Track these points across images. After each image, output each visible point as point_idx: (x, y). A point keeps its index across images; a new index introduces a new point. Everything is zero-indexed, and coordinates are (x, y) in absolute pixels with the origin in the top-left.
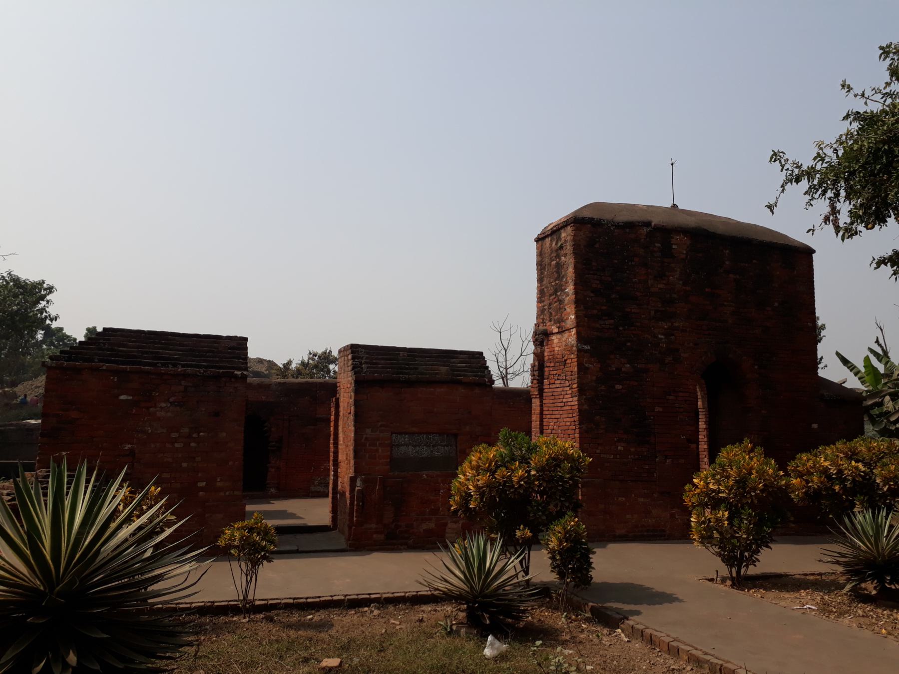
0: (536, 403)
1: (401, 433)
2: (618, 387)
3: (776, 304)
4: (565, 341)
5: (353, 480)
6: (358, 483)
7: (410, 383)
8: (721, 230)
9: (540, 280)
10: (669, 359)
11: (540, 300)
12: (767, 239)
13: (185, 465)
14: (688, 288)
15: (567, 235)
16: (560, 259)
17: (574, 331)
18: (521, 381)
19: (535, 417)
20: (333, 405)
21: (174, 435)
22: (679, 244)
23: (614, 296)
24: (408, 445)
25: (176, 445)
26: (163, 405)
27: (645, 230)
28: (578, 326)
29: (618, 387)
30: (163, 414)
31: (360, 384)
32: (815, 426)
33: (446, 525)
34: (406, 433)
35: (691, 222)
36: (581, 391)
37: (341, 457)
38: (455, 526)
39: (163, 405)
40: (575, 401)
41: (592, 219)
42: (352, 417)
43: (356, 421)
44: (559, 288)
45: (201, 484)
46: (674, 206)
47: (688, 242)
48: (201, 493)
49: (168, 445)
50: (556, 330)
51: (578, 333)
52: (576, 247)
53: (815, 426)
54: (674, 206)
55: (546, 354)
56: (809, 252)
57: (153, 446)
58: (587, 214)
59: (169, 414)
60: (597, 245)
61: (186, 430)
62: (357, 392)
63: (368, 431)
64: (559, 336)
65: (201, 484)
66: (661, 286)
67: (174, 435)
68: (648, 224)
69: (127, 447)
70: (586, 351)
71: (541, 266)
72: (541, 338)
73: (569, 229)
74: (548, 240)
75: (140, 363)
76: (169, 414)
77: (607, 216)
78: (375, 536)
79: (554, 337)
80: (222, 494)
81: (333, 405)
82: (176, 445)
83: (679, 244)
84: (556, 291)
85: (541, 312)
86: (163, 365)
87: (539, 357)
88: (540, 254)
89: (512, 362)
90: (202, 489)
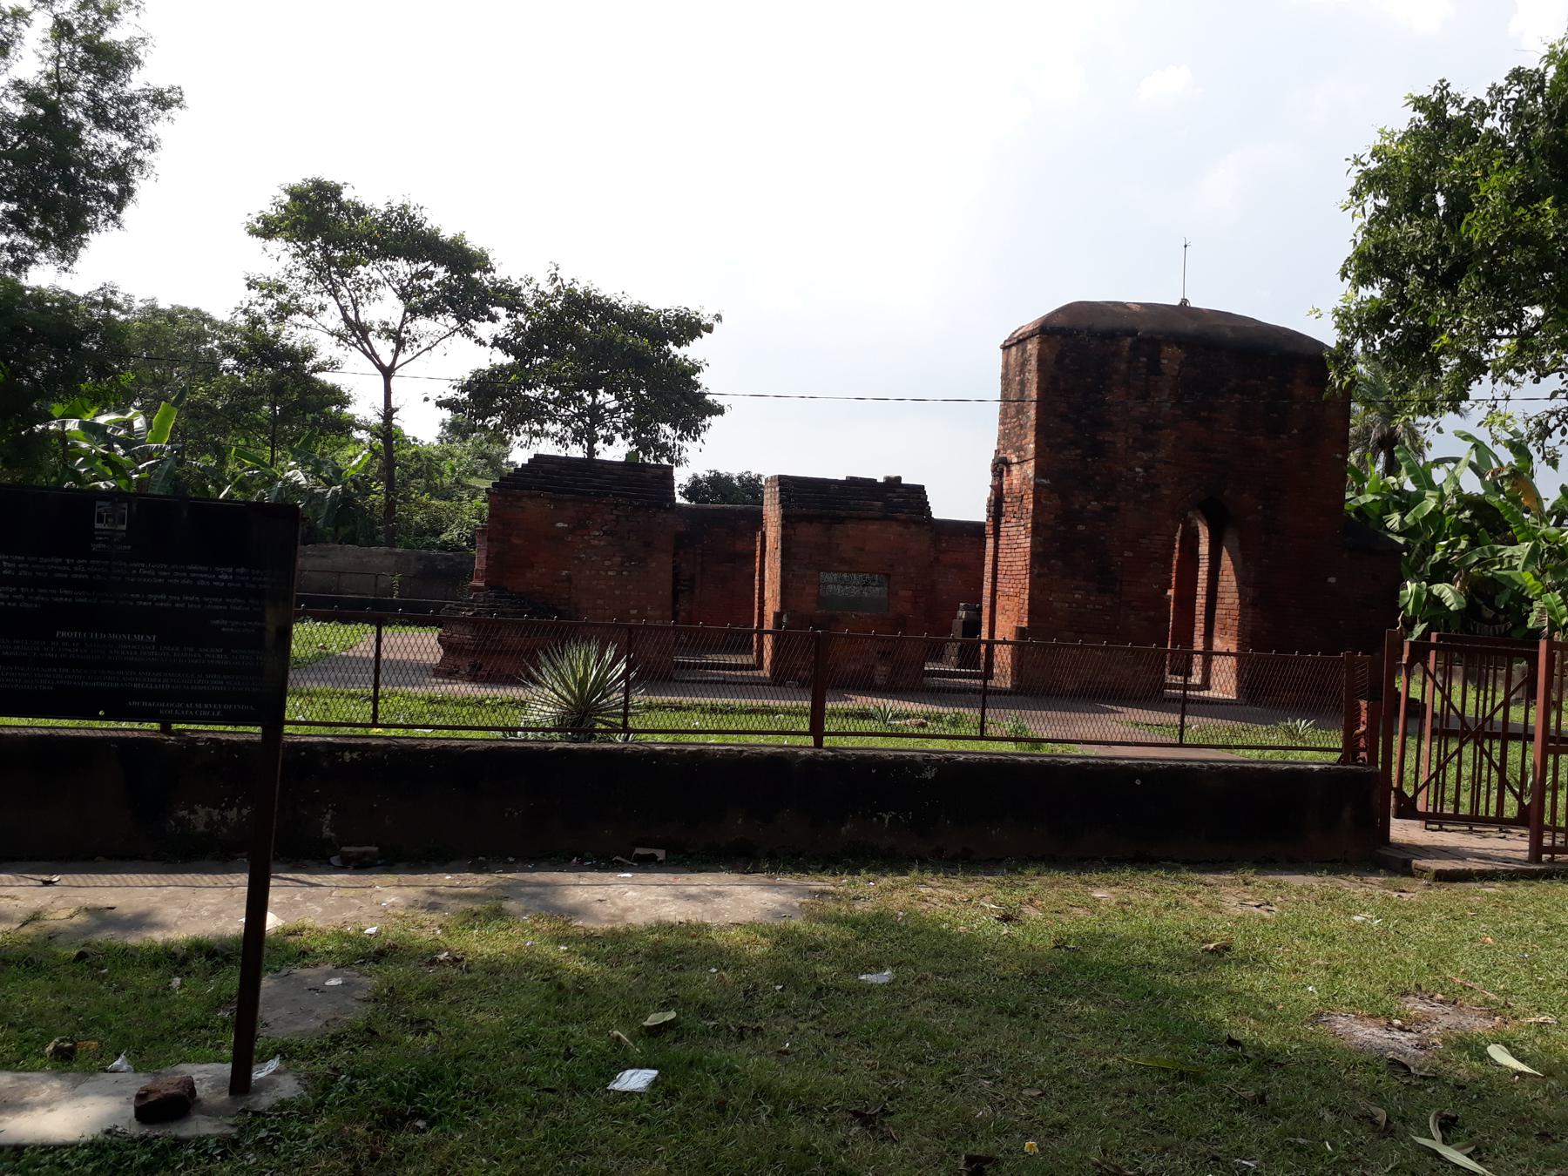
0: (990, 543)
2: (1081, 527)
4: (1022, 474)
5: (778, 616)
7: (842, 520)
10: (1145, 496)
11: (1002, 423)
15: (1032, 347)
17: (1032, 463)
18: (978, 512)
19: (988, 560)
20: (759, 538)
21: (607, 563)
22: (1171, 358)
27: (1129, 340)
28: (1037, 456)
31: (787, 521)
32: (1332, 580)
35: (1191, 326)
36: (1036, 532)
37: (767, 595)
40: (1027, 543)
42: (779, 553)
43: (783, 556)
44: (1020, 411)
46: (1185, 301)
47: (1183, 356)
51: (1036, 466)
52: (1040, 360)
53: (1332, 580)
54: (1185, 301)
58: (1060, 322)
60: (1067, 361)
62: (783, 527)
67: (607, 563)
68: (1132, 333)
70: (1045, 486)
71: (1005, 377)
72: (1000, 467)
73: (1035, 340)
74: (1014, 349)
81: (759, 538)
83: (1171, 358)
85: (1004, 436)
87: (998, 491)
88: (1006, 365)
89: (958, 496)
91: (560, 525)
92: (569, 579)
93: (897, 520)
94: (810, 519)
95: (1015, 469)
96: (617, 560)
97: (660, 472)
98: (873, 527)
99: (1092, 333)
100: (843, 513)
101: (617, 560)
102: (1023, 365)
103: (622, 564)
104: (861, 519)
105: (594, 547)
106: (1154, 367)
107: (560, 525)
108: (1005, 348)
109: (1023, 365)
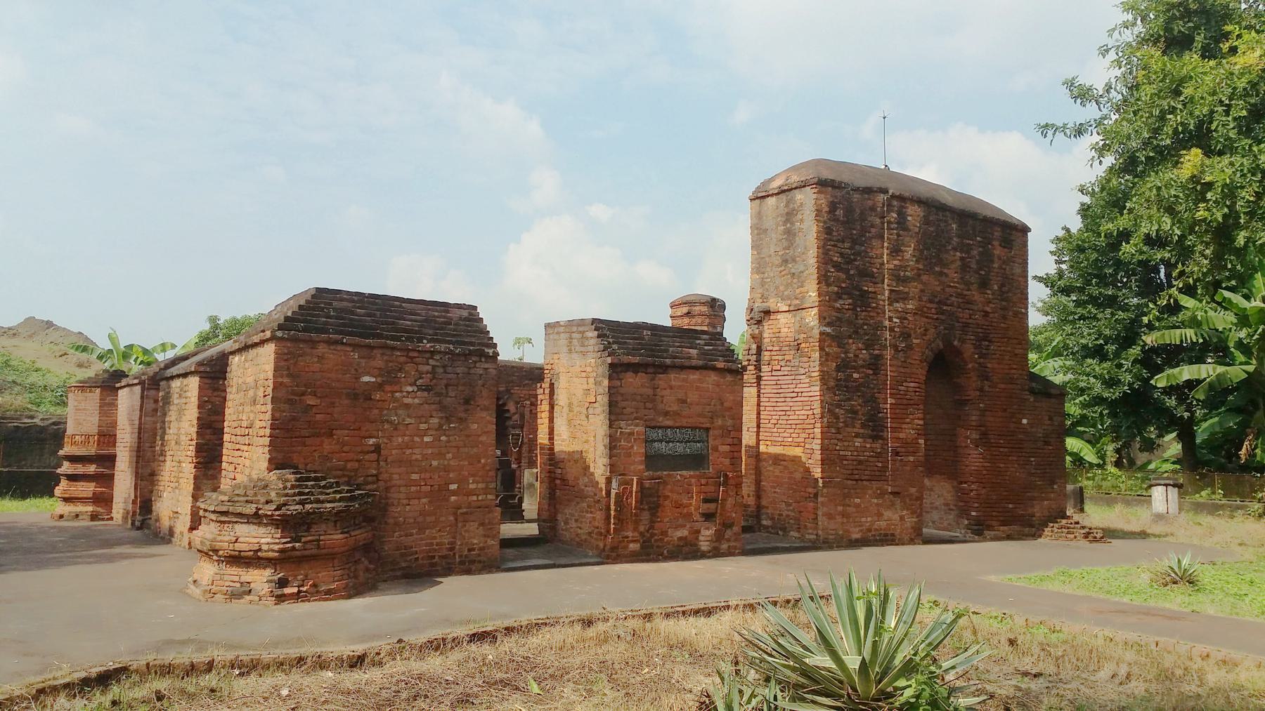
1: (653, 428)
2: (855, 375)
3: (996, 287)
6: (614, 484)
7: (665, 369)
8: (950, 201)
9: (756, 246)
12: (989, 214)
13: (435, 463)
14: (921, 267)
16: (793, 224)
17: (815, 311)
21: (423, 426)
23: (852, 272)
24: (661, 441)
25: (426, 439)
26: (410, 389)
29: (855, 375)
30: (407, 401)
32: (1025, 421)
33: (698, 532)
34: (660, 427)
38: (708, 533)
39: (410, 389)
41: (833, 181)
45: (453, 487)
48: (453, 498)
49: (417, 439)
50: (786, 308)
55: (765, 335)
56: (1025, 230)
57: (400, 439)
59: (416, 401)
61: (436, 421)
63: (623, 424)
64: (788, 315)
65: (453, 487)
66: (896, 262)
67: (423, 426)
68: (885, 191)
69: (372, 441)
70: (828, 334)
74: (771, 201)
75: (380, 336)
76: (416, 401)
77: (845, 177)
78: (631, 545)
79: (779, 316)
80: (475, 498)
82: (426, 439)
84: (785, 261)
86: (408, 339)
90: (454, 493)
91: (366, 379)
92: (377, 449)
93: (714, 369)
94: (635, 368)
95: (783, 319)
96: (435, 421)
97: (465, 313)
98: (694, 376)
99: (857, 190)
100: (668, 361)
101: (435, 421)
102: (790, 215)
103: (441, 426)
104: (683, 368)
105: (407, 406)
106: (902, 222)
107: (366, 379)
108: (760, 197)
109: (790, 215)
